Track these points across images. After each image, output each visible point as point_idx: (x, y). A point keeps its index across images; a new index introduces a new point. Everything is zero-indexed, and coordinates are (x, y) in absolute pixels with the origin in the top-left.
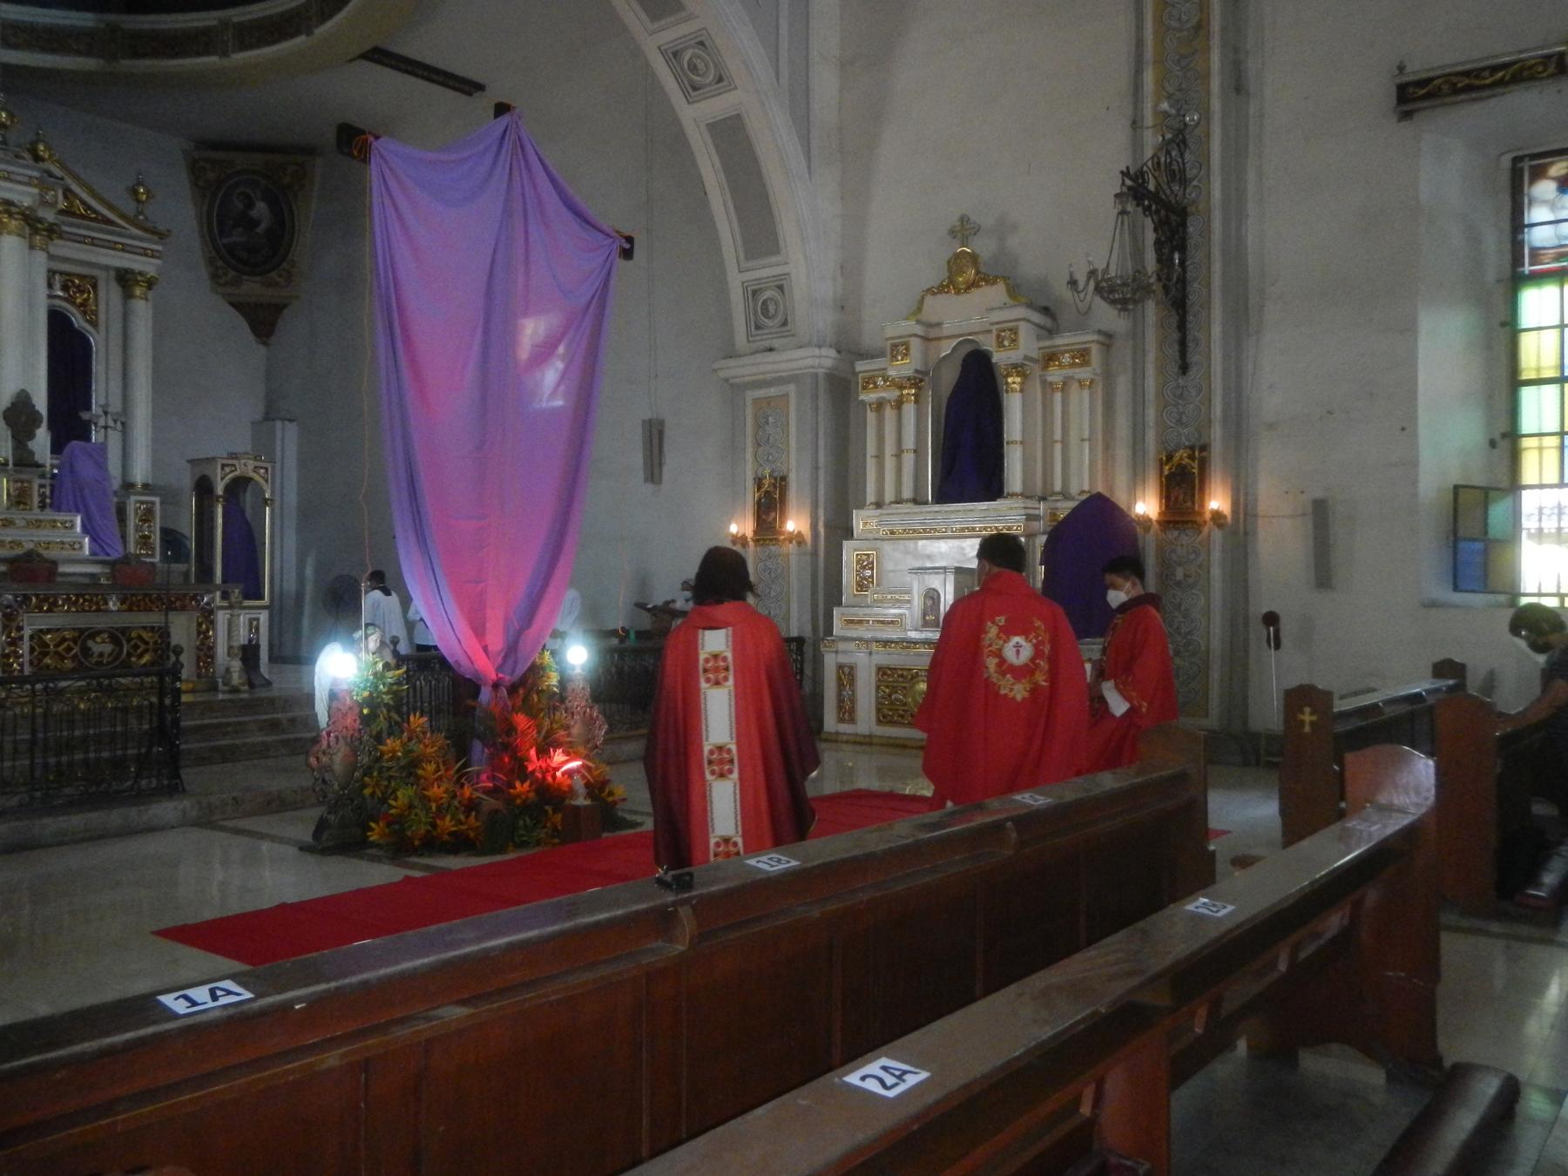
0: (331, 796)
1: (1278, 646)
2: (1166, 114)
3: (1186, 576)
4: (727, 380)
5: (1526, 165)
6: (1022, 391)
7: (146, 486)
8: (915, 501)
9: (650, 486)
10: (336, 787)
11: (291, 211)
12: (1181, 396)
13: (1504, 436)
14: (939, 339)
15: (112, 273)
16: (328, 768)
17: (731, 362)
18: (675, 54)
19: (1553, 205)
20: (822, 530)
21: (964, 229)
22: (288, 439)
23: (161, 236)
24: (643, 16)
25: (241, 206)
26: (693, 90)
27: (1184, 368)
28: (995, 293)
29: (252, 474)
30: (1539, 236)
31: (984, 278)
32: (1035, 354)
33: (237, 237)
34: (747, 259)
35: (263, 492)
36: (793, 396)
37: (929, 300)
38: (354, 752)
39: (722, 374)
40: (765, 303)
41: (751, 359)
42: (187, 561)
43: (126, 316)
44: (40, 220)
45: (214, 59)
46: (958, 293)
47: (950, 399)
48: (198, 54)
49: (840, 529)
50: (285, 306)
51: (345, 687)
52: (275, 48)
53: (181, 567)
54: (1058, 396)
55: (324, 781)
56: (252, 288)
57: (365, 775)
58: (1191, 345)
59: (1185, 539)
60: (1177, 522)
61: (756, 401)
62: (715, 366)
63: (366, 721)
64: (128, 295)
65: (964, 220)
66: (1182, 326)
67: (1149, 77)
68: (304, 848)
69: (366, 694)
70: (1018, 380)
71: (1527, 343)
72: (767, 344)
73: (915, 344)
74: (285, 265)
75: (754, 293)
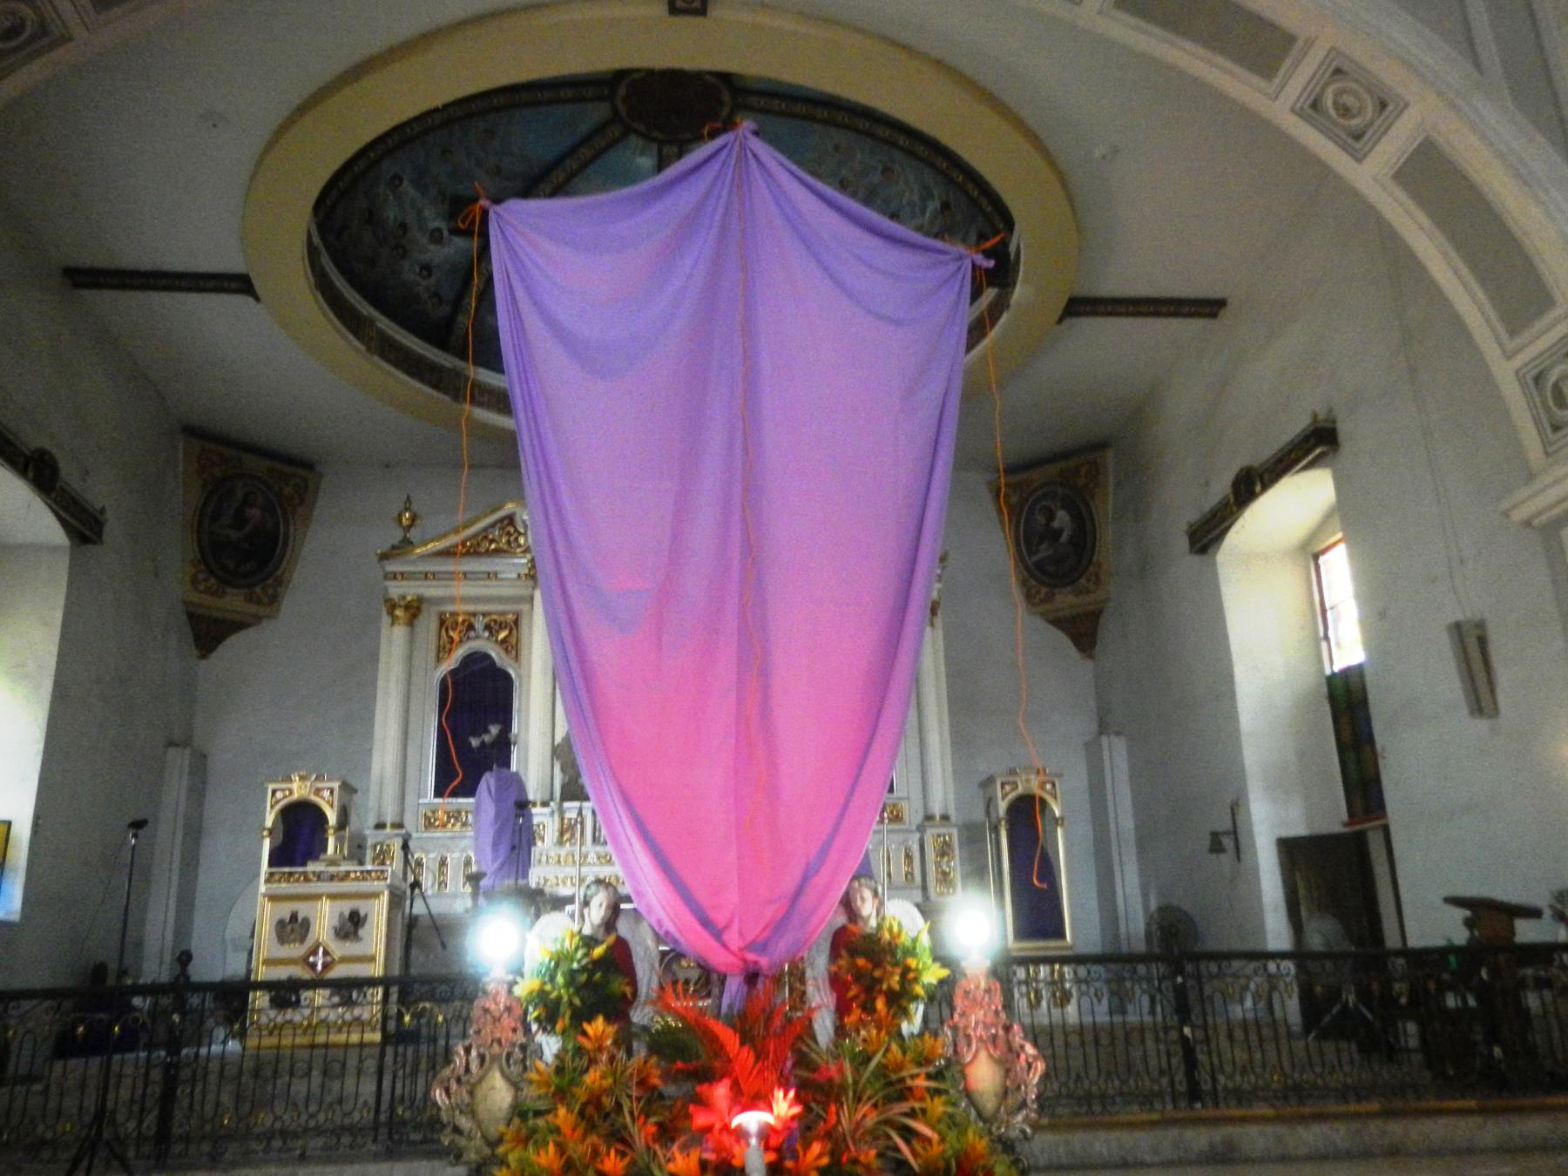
4: (1528, 523)
7: (945, 818)
9: (1481, 726)
11: (1091, 513)
18: (1315, 105)
22: (1117, 754)
24: (1255, 79)
25: (1041, 519)
26: (1356, 140)
29: (1038, 792)
33: (1045, 551)
34: (1513, 333)
39: (1519, 515)
40: (1557, 388)
56: (1066, 600)
62: (1505, 505)
74: (1092, 569)
75: (1538, 379)
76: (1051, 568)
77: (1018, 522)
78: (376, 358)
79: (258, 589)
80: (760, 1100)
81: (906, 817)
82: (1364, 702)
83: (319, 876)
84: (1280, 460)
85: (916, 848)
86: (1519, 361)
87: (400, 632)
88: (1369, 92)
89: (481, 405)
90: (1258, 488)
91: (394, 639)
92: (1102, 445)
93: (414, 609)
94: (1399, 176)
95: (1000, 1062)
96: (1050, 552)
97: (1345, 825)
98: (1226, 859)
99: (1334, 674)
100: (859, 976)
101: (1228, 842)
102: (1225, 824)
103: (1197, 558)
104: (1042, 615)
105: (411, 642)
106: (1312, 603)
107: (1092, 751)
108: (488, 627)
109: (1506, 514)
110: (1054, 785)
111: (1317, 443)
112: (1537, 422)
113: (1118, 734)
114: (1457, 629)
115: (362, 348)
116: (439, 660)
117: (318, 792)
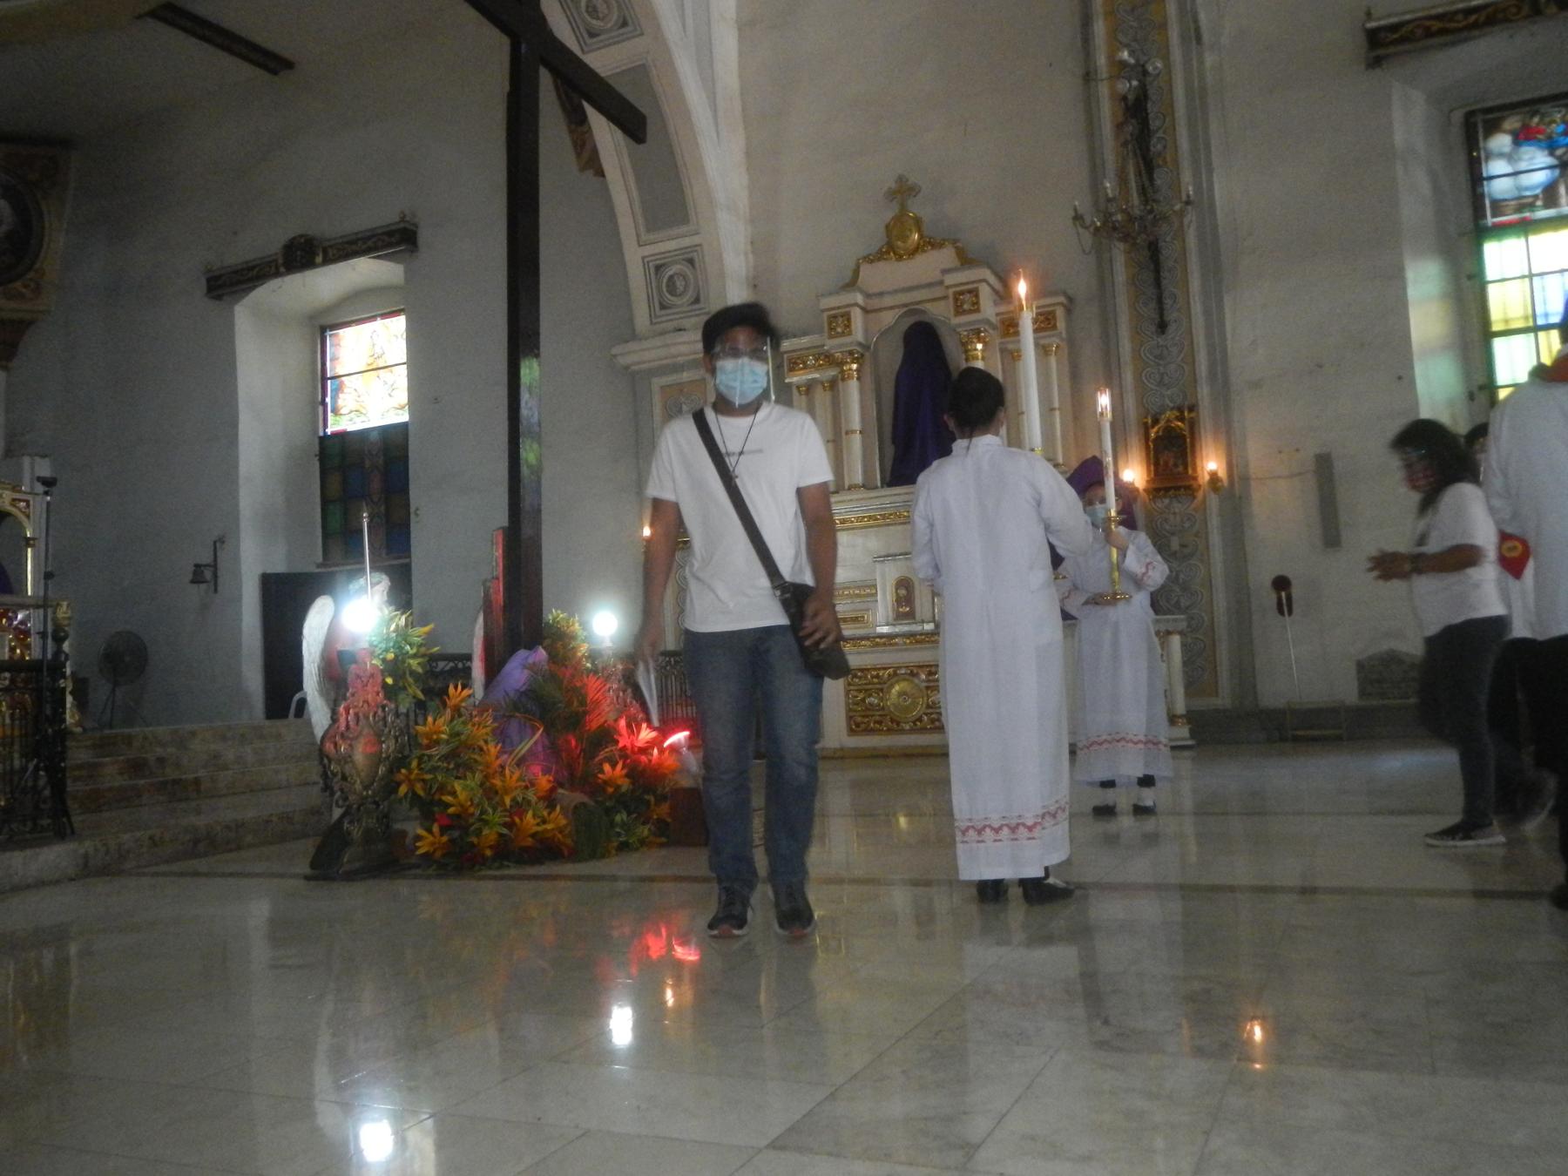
0: (352, 798)
1: (1290, 612)
2: (1123, 64)
3: (1183, 546)
4: (627, 368)
5: (1479, 118)
10: (358, 786)
12: (1160, 357)
13: (1481, 388)
14: (880, 310)
16: (347, 759)
17: (632, 346)
19: (1509, 158)
21: (903, 191)
27: (1162, 327)
28: (946, 256)
30: (1500, 188)
32: (994, 319)
34: (648, 231)
35: (23, 529)
37: (866, 270)
38: (379, 737)
39: (622, 361)
40: (671, 277)
41: (657, 342)
46: (900, 258)
50: (31, 323)
51: (365, 645)
55: (344, 778)
57: (391, 771)
58: (1168, 302)
59: (1177, 507)
60: (1167, 490)
62: (614, 351)
63: (390, 692)
65: (901, 179)
66: (1158, 283)
67: (1100, 28)
68: (307, 878)
69: (391, 656)
70: (979, 346)
71: (1494, 294)
73: (857, 317)
74: (31, 275)
75: (658, 268)
86: (648, 250)
88: (619, 6)
90: (319, 259)
97: (319, 566)
101: (208, 574)
102: (206, 558)
106: (314, 371)
110: (27, 502)
111: (398, 239)
112: (649, 299)
113: (43, 456)
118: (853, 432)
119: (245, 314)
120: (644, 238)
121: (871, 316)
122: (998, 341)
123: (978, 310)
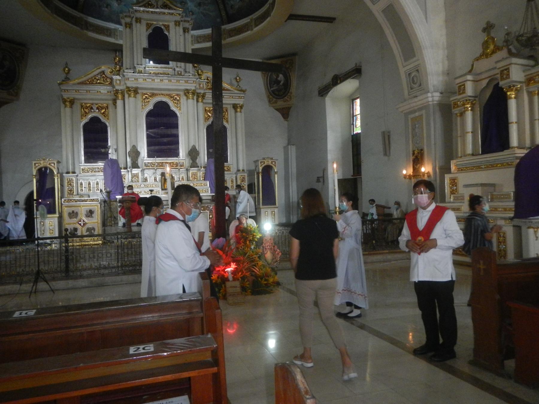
4: (402, 112)
6: (515, 98)
7: (243, 170)
8: (473, 155)
9: (386, 158)
11: (290, 76)
15: (232, 106)
20: (438, 170)
21: (488, 28)
22: (293, 150)
23: (244, 91)
28: (503, 53)
31: (498, 49)
33: (275, 88)
34: (406, 60)
36: (424, 117)
37: (475, 63)
39: (401, 110)
42: (255, 193)
43: (236, 117)
44: (200, 93)
45: (249, 32)
46: (487, 57)
47: (484, 107)
48: (246, 31)
49: (446, 169)
52: (263, 23)
53: (254, 195)
54: (536, 97)
56: (281, 103)
61: (412, 119)
64: (236, 112)
65: (488, 23)
72: (414, 95)
74: (289, 94)
75: (409, 74)
76: (277, 93)
77: (267, 78)
78: (55, 15)
79: (11, 91)
80: (228, 265)
81: (232, 170)
82: (360, 144)
83: (79, 201)
84: (345, 75)
85: (234, 179)
87: (68, 109)
89: (90, 31)
90: (339, 82)
91: (66, 112)
92: (294, 54)
93: (72, 102)
94: (384, 11)
95: (272, 253)
96: (277, 88)
97: (352, 176)
98: (320, 184)
99: (354, 135)
100: (243, 237)
101: (321, 180)
103: (320, 98)
104: (273, 107)
105: (72, 112)
107: (286, 149)
108: (97, 108)
109: (397, 109)
113: (293, 145)
114: (383, 133)
115: (50, 11)
116: (82, 118)
117: (50, 164)
118: (468, 132)
119: (328, 100)
120: (404, 64)
121: (480, 82)
122: (525, 88)
123: (509, 78)
